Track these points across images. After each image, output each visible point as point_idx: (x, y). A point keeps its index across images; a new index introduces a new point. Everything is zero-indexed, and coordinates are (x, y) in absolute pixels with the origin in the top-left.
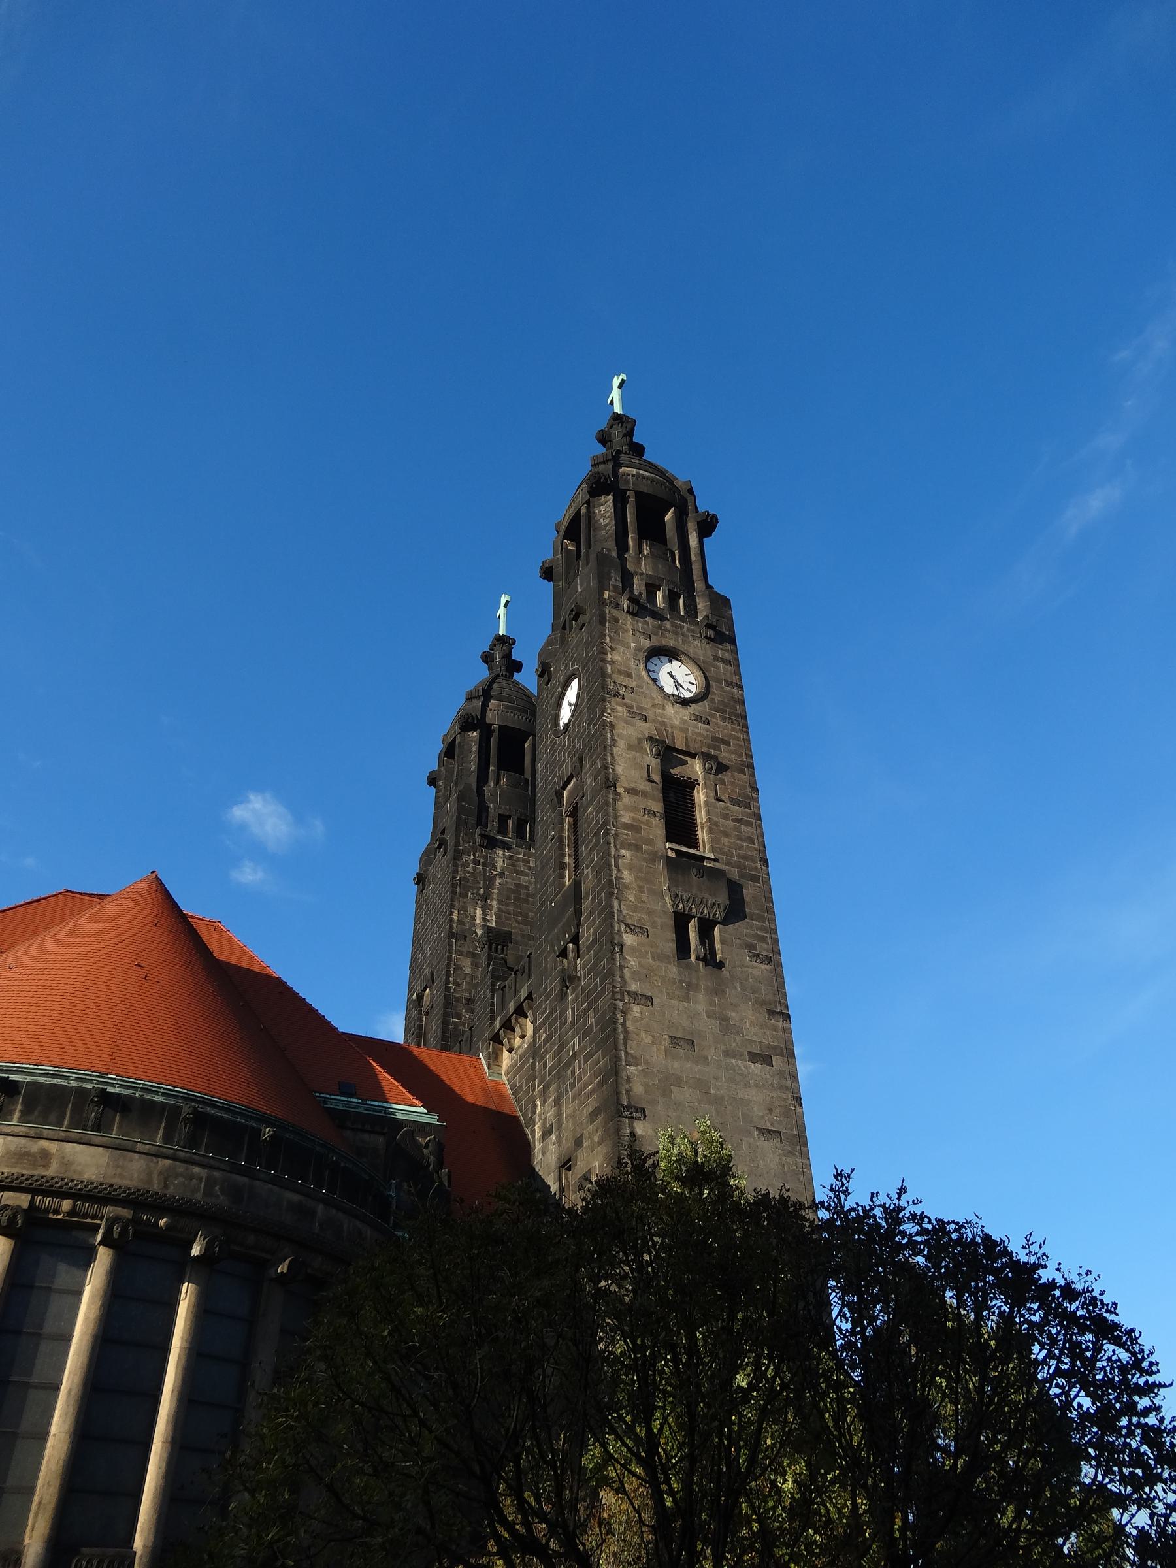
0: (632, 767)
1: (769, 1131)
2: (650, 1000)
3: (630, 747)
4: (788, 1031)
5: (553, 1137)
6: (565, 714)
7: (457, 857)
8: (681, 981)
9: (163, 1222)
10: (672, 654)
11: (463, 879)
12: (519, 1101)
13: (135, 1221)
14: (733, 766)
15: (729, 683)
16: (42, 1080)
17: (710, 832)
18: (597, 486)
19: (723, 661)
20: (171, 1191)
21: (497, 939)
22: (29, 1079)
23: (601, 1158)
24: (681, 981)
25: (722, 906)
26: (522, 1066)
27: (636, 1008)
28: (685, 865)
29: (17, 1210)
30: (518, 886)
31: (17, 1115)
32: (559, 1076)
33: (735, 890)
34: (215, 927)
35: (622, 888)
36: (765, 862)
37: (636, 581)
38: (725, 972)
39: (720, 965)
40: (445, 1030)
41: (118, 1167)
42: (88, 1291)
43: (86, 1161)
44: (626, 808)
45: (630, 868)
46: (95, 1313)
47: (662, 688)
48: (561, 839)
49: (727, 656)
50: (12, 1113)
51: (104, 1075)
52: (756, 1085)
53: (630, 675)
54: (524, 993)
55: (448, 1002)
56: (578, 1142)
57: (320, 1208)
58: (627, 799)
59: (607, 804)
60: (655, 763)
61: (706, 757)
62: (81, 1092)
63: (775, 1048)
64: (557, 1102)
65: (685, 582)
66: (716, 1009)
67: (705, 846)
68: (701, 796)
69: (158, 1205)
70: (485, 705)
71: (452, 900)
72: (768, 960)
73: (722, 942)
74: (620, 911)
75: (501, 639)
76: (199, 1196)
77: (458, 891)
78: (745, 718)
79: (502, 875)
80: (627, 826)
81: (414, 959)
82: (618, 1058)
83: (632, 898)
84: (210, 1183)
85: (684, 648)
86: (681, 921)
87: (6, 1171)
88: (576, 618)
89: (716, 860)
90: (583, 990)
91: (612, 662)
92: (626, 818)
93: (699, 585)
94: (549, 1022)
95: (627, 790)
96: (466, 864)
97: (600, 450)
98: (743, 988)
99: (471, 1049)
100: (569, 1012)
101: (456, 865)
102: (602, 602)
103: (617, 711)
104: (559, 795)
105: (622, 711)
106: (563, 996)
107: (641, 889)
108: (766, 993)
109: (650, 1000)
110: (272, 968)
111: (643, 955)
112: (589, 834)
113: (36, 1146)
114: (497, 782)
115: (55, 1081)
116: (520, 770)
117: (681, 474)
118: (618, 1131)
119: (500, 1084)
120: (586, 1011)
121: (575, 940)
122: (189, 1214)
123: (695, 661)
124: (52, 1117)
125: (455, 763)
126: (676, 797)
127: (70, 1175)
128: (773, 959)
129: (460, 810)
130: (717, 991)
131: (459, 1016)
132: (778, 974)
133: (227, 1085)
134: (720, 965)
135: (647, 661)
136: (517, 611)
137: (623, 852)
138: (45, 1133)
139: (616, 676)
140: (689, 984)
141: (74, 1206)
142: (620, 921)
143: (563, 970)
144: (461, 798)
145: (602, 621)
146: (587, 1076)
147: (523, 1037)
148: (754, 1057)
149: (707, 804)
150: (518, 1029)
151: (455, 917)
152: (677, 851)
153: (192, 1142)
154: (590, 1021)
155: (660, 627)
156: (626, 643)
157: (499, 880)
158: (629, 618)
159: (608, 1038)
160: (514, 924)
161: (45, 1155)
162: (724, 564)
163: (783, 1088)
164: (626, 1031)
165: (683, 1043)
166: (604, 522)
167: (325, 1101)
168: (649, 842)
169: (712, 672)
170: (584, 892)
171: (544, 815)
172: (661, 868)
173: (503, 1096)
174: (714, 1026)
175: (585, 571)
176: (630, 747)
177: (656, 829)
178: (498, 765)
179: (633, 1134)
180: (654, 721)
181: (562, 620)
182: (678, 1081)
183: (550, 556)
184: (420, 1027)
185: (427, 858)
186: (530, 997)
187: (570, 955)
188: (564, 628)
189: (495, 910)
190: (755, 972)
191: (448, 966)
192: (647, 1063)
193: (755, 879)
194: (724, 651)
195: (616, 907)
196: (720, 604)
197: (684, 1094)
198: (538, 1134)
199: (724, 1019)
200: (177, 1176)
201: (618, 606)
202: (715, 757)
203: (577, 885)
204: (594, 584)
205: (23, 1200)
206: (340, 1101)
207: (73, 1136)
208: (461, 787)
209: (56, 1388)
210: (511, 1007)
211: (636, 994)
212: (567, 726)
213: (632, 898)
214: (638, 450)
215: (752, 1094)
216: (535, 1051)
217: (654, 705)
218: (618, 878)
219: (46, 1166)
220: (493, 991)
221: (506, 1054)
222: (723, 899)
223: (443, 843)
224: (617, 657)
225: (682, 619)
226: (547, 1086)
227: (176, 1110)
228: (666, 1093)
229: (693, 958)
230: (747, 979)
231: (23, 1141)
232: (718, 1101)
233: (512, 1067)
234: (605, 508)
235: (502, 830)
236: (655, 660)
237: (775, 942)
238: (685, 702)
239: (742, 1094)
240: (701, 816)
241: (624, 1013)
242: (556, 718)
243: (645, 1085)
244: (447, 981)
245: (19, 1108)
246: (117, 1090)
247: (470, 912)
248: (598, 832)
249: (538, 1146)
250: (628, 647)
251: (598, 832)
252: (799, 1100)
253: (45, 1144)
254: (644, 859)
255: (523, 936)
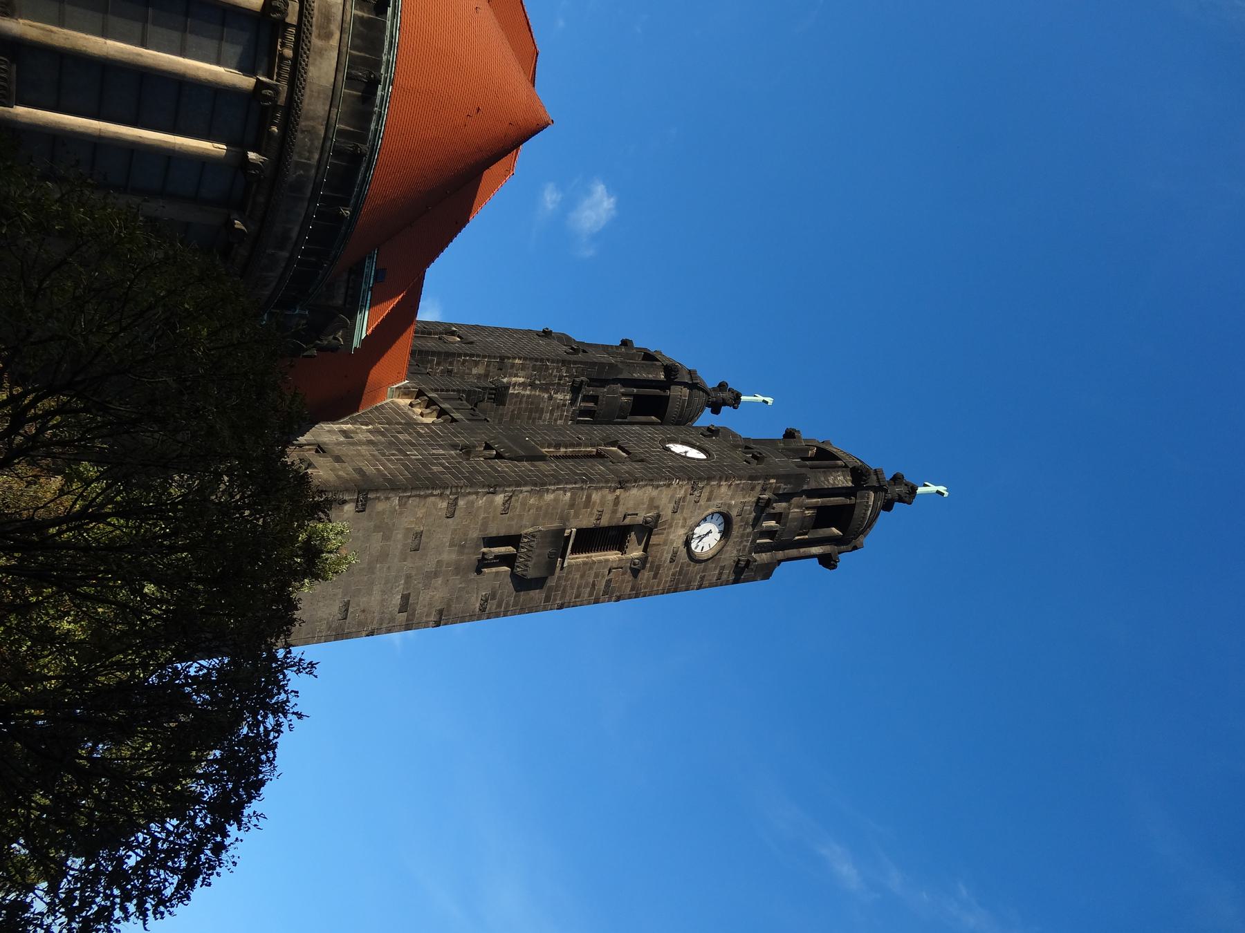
0: (636, 501)
1: (347, 610)
2: (452, 516)
3: (652, 500)
4: (426, 625)
5: (342, 439)
6: (678, 448)
7: (564, 362)
8: (466, 540)
9: (275, 129)
10: (726, 534)
11: (547, 368)
12: (371, 412)
13: (276, 107)
14: (636, 582)
15: (702, 578)
16: (388, 33)
17: (585, 564)
18: (859, 474)
19: (720, 574)
20: (300, 135)
21: (499, 395)
22: (389, 23)
23: (325, 477)
24: (466, 540)
25: (526, 573)
26: (398, 414)
27: (445, 505)
28: (558, 543)
29: (284, 13)
30: (542, 411)
31: (360, 13)
32: (391, 444)
33: (539, 583)
34: (509, 170)
35: (540, 494)
36: (561, 607)
37: (784, 504)
38: (473, 575)
39: (479, 571)
40: (427, 353)
42: (220, 69)
43: (323, 69)
44: (603, 497)
45: (556, 500)
46: (203, 75)
47: (698, 525)
48: (579, 445)
49: (724, 577)
50: (361, 9)
51: (392, 83)
52: (383, 600)
53: (709, 499)
54: (456, 415)
55: (449, 355)
56: (338, 459)
57: (285, 254)
58: (611, 497)
59: (607, 481)
60: (639, 520)
61: (644, 560)
62: (378, 64)
63: (413, 614)
64: (370, 442)
65: (782, 543)
66: (444, 568)
67: (572, 559)
68: (613, 556)
69: (289, 125)
70: (685, 384)
71: (531, 359)
72: (483, 609)
73: (497, 573)
74: (521, 492)
75: (737, 397)
76: (295, 158)
77: (538, 364)
78: (675, 591)
79: (550, 398)
80: (589, 497)
81: (483, 328)
82: (405, 490)
83: (532, 501)
84: (306, 167)
85: (730, 543)
86: (513, 540)
87: (315, 5)
88: (754, 457)
89: (562, 568)
90: (459, 463)
91: (720, 486)
92: (596, 497)
93: (780, 554)
94: (433, 436)
95: (618, 497)
96: (559, 370)
97: (888, 476)
98: (461, 589)
99: (411, 374)
100: (442, 452)
101: (558, 361)
102: (767, 478)
103: (680, 489)
104: (613, 444)
105: (680, 494)
106: (454, 447)
107: (539, 508)
108: (456, 608)
109: (452, 516)
110: (476, 216)
111: (488, 510)
112: (583, 467)
113: (335, 29)
114: (624, 395)
115: (387, 43)
116: (633, 413)
117: (869, 541)
118: (347, 490)
119: (384, 397)
120: (442, 465)
121: (499, 456)
122: (281, 150)
123: (720, 551)
124: (358, 42)
125: (639, 361)
126: (613, 537)
127: (312, 55)
128: (484, 613)
129: (602, 365)
130: (458, 569)
131: (438, 364)
132: (472, 617)
133: (384, 180)
134: (479, 571)
135: (721, 513)
136: (759, 410)
137: (569, 494)
139: (708, 489)
140: (463, 546)
141: (287, 59)
142: (514, 492)
143: (475, 447)
144: (611, 365)
145: (752, 478)
146: (390, 466)
147: (422, 415)
148: (405, 598)
149: (607, 561)
150: (428, 411)
151: (517, 361)
152: (569, 537)
153: (338, 153)
154: (435, 468)
155: (747, 523)
156: (735, 497)
158: (754, 499)
159: (420, 483)
160: (512, 408)
161: (328, 36)
162: (797, 575)
163: (381, 621)
164: (426, 496)
165: (417, 543)
166: (831, 479)
167: (371, 258)
168: (576, 515)
169: (711, 565)
170: (537, 463)
171: (598, 432)
172: (556, 525)
173: (374, 399)
174: (430, 566)
175: (791, 464)
176: (652, 500)
177: (587, 521)
178: (638, 395)
179: (344, 502)
180: (673, 519)
181: (752, 445)
182: (386, 538)
183: (803, 437)
184: (430, 333)
185: (564, 339)
186: (454, 420)
187: (487, 452)
188: (747, 447)
190: (473, 599)
191: (478, 356)
192: (401, 513)
193: (547, 599)
194: (728, 574)
195: (525, 489)
196: (766, 572)
197: (376, 542)
198: (344, 427)
199: (436, 574)
201: (764, 490)
202: (644, 567)
203: (542, 458)
204: (782, 471)
205: (292, 18)
206: (371, 270)
207: (343, 58)
208: (620, 366)
209: (143, 44)
210: (445, 406)
211: (456, 504)
212: (668, 449)
213: (532, 501)
214: (888, 506)
215: (376, 596)
216: (410, 424)
217: (685, 519)
218: (548, 490)
219: (319, 36)
220: (458, 391)
221: (408, 401)
222: (531, 573)
223: (576, 351)
224: (724, 489)
225: (754, 541)
226: (382, 434)
227: (364, 141)
228: (377, 528)
229: (484, 550)
230: (468, 593)
231: (339, 18)
232: (371, 570)
233: (398, 406)
234: (842, 480)
235: (587, 398)
236: (721, 520)
237: (497, 615)
238: (687, 543)
239: (376, 590)
240: (597, 556)
241: (441, 495)
242: (675, 441)
243: (383, 512)
244: (466, 355)
245: (366, 15)
246: (379, 93)
247: (521, 373)
248: (584, 474)
249: (335, 427)
250: (732, 498)
251: (584, 474)
252: (371, 634)
253: (337, 36)
254: (563, 511)
255: (502, 415)
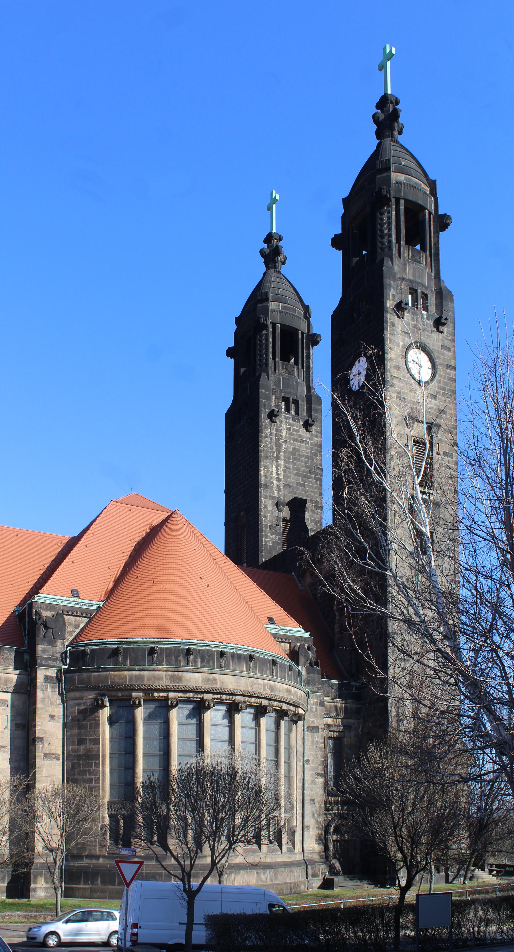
16: (203, 648)
20: (254, 690)
41: (237, 682)
50: (197, 662)
76: (262, 691)
124: (211, 663)
138: (214, 672)
157: (284, 446)
161: (215, 679)
189: (282, 467)
200: (255, 684)
219: (216, 684)
245: (199, 660)
247: (270, 470)
